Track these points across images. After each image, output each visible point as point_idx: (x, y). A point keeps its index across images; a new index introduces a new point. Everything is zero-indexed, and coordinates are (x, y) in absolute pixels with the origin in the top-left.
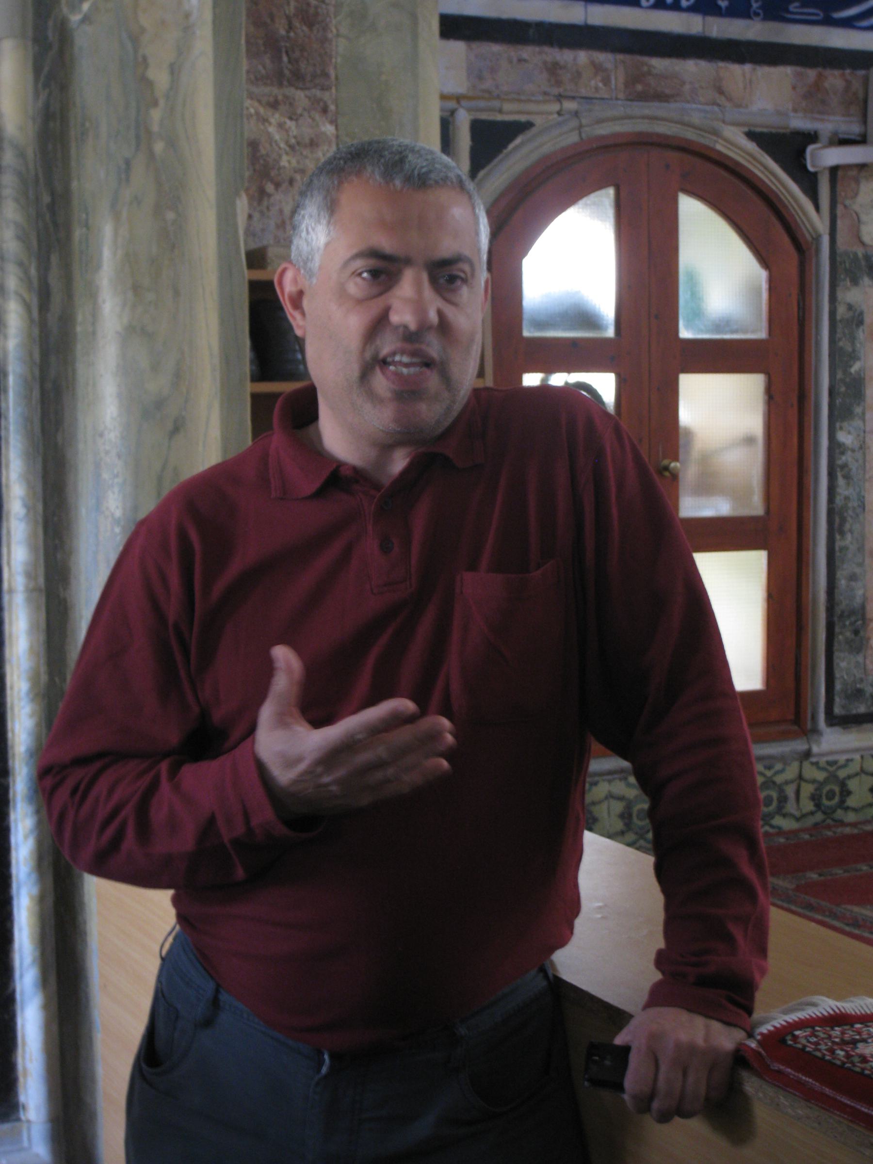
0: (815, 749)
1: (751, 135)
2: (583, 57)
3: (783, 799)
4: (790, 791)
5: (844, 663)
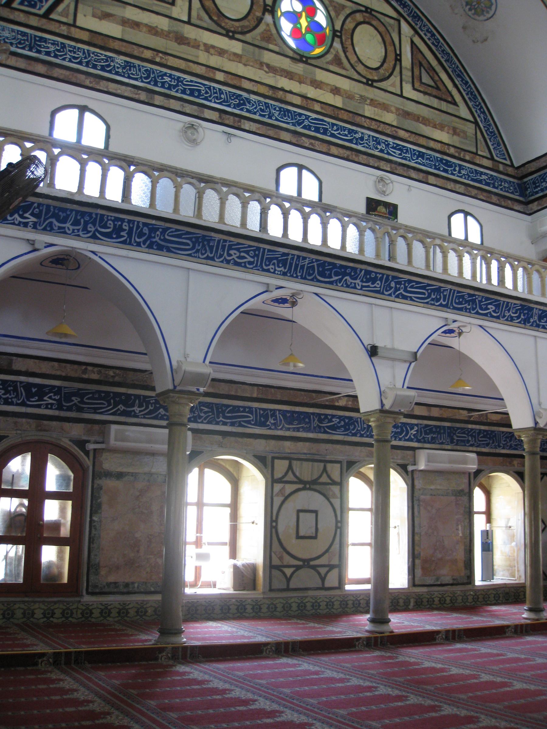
0: (82, 600)
1: (70, 440)
2: (24, 420)
3: (72, 613)
4: (74, 611)
5: (92, 578)
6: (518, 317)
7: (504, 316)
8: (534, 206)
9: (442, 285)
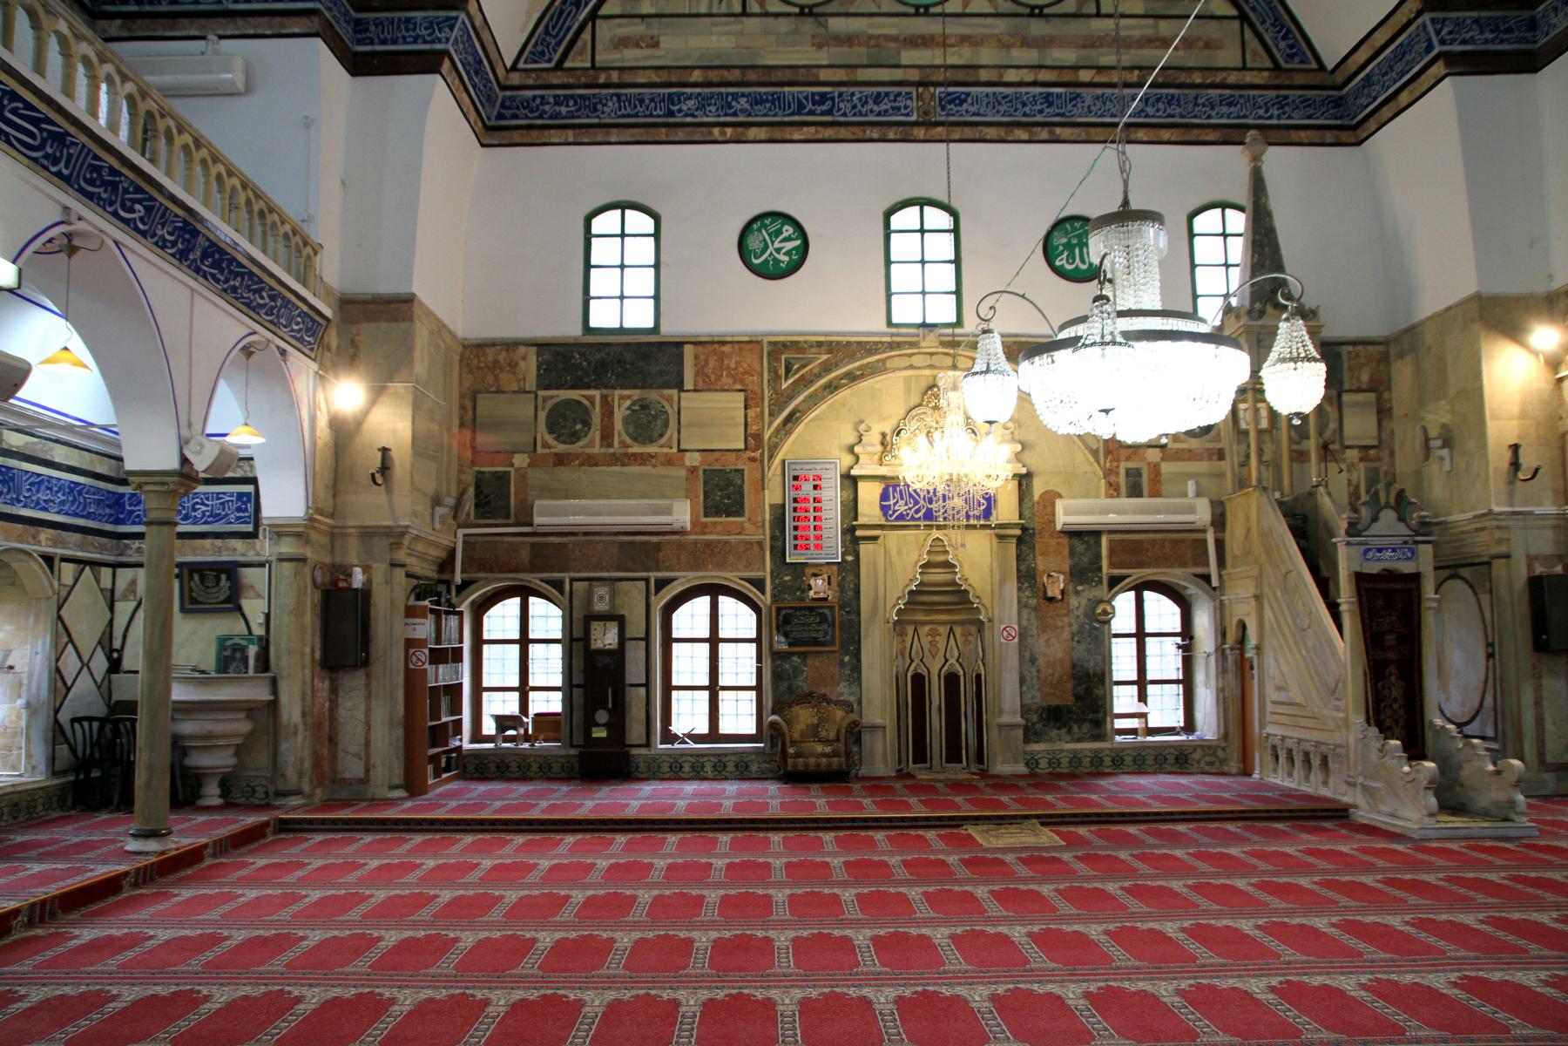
6: (174, 244)
7: (154, 235)
8: (114, 27)
9: (72, 130)
